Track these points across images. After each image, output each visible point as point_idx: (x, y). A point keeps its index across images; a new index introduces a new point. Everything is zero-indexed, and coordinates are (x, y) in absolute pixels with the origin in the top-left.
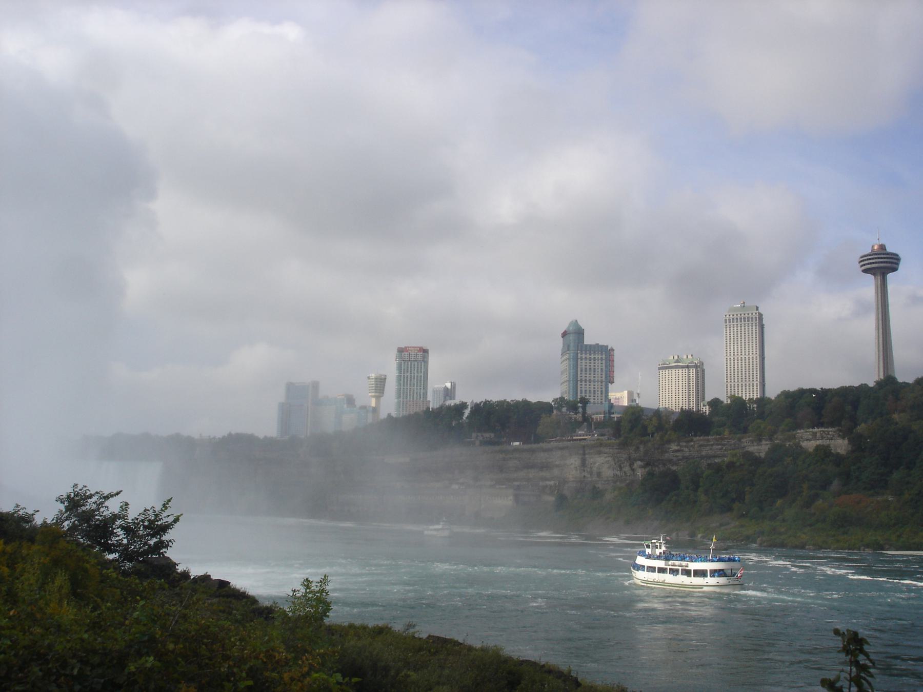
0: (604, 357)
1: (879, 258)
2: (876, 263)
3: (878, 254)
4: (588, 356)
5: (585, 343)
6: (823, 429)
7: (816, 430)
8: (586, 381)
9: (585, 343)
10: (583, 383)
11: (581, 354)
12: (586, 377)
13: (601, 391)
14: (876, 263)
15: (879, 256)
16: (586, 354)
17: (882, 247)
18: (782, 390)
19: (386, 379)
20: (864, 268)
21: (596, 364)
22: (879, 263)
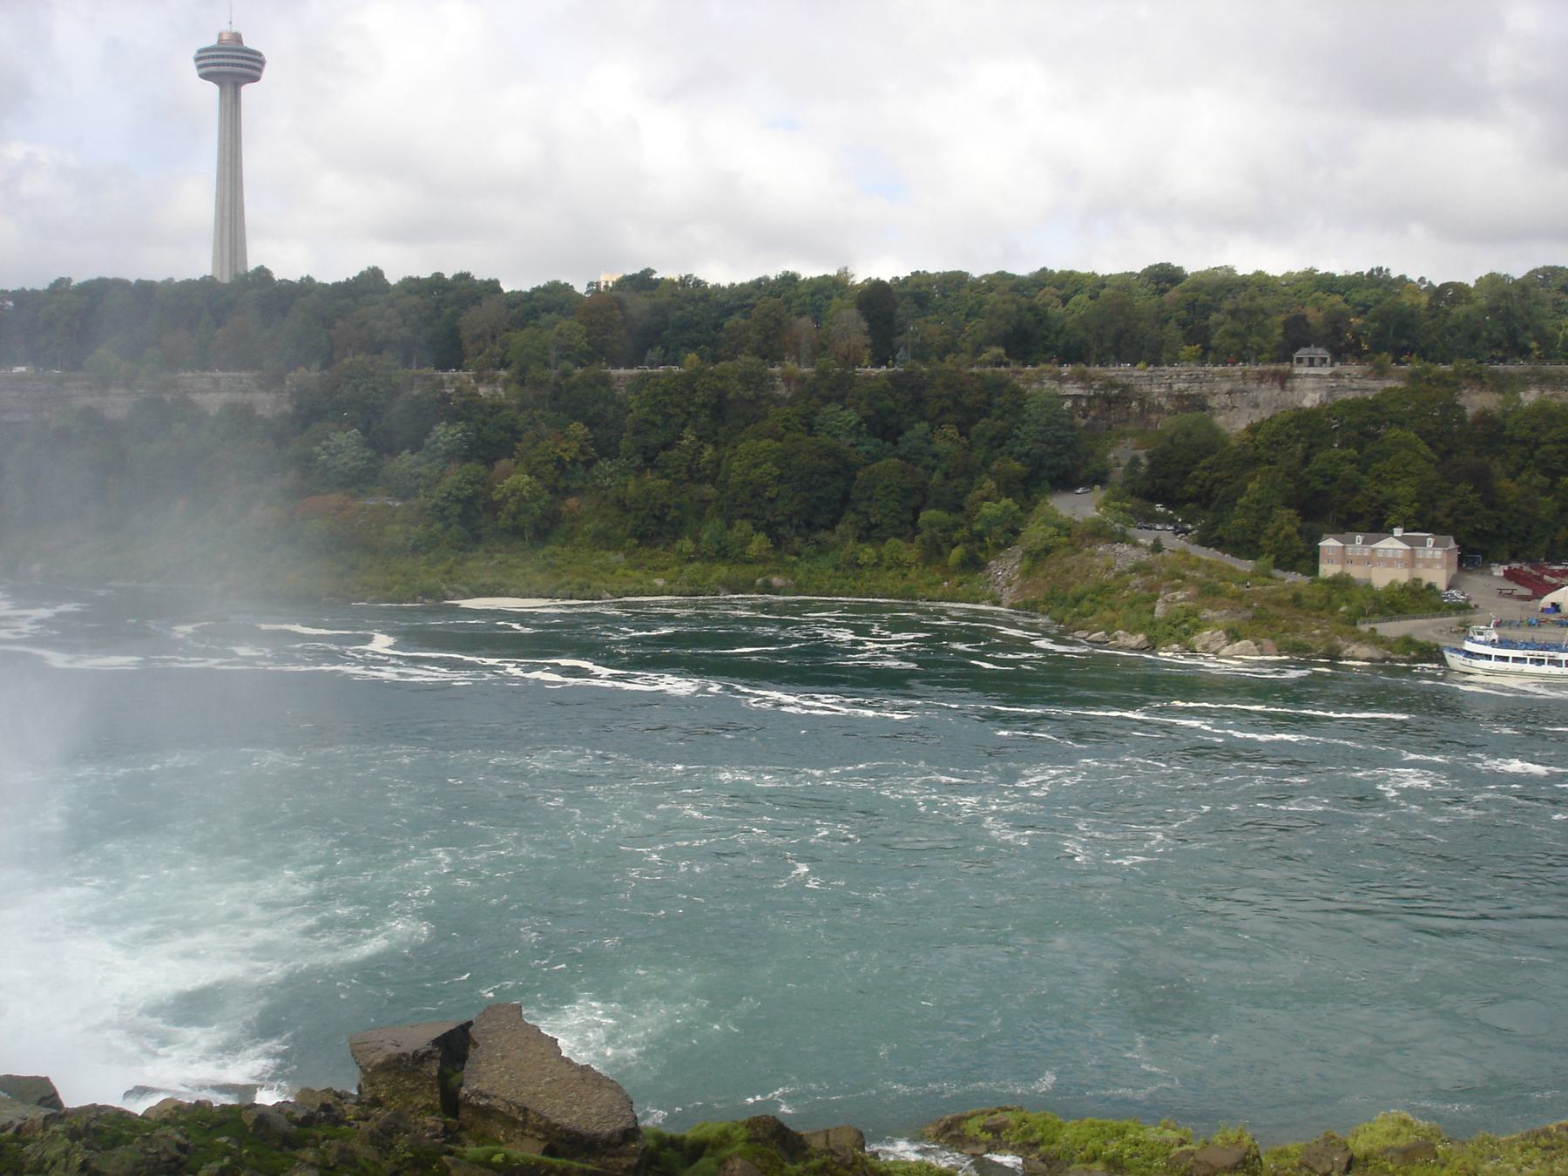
1: (233, 57)
2: (228, 65)
3: (232, 50)
6: (231, 374)
7: (218, 374)
14: (228, 65)
15: (234, 54)
17: (237, 38)
18: (57, 278)
20: (204, 70)
22: (233, 65)
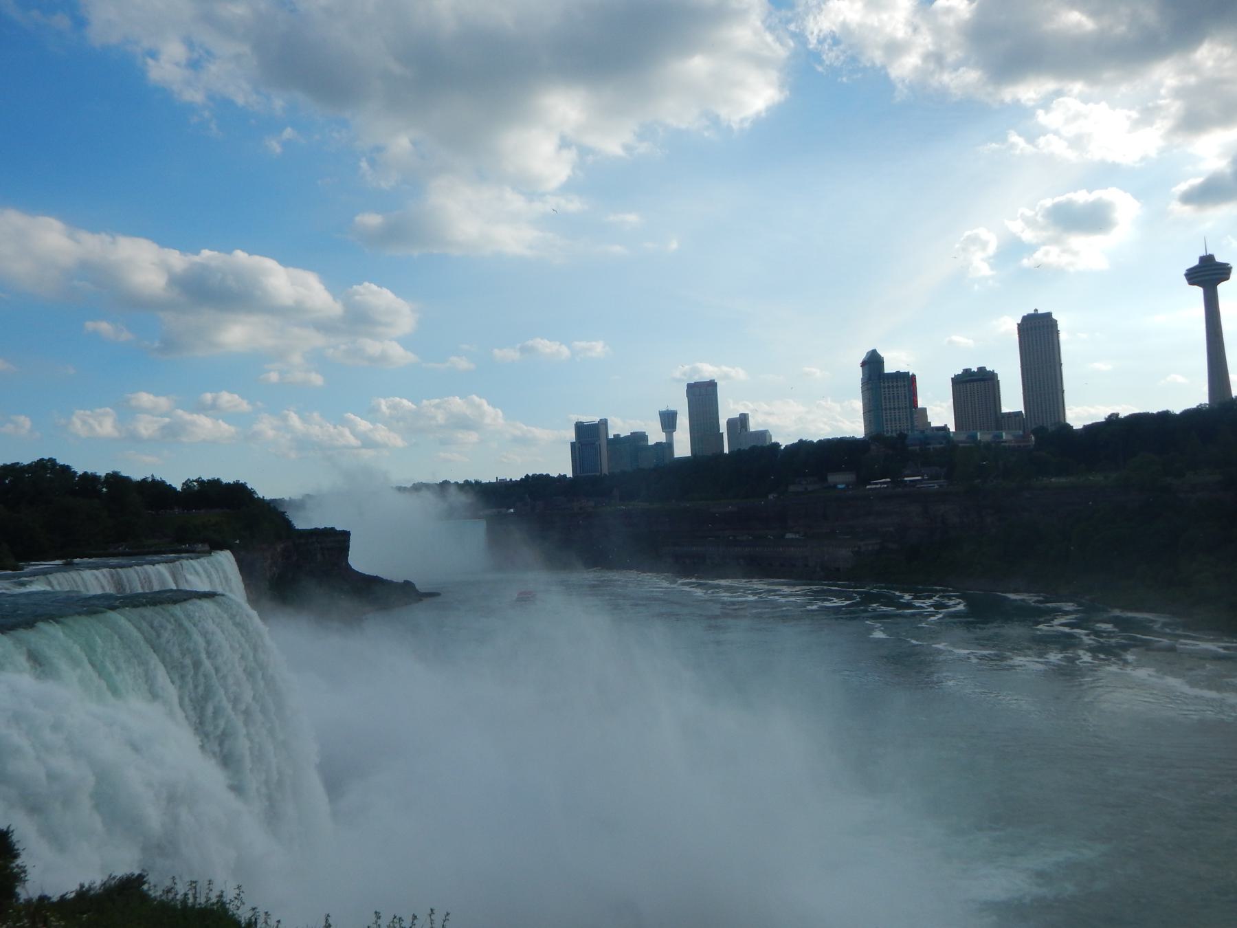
0: (906, 383)
4: (891, 384)
5: (886, 371)
8: (890, 409)
9: (886, 371)
10: (888, 412)
11: (884, 383)
12: (890, 405)
13: (907, 418)
16: (888, 383)
19: (677, 413)
21: (899, 392)
